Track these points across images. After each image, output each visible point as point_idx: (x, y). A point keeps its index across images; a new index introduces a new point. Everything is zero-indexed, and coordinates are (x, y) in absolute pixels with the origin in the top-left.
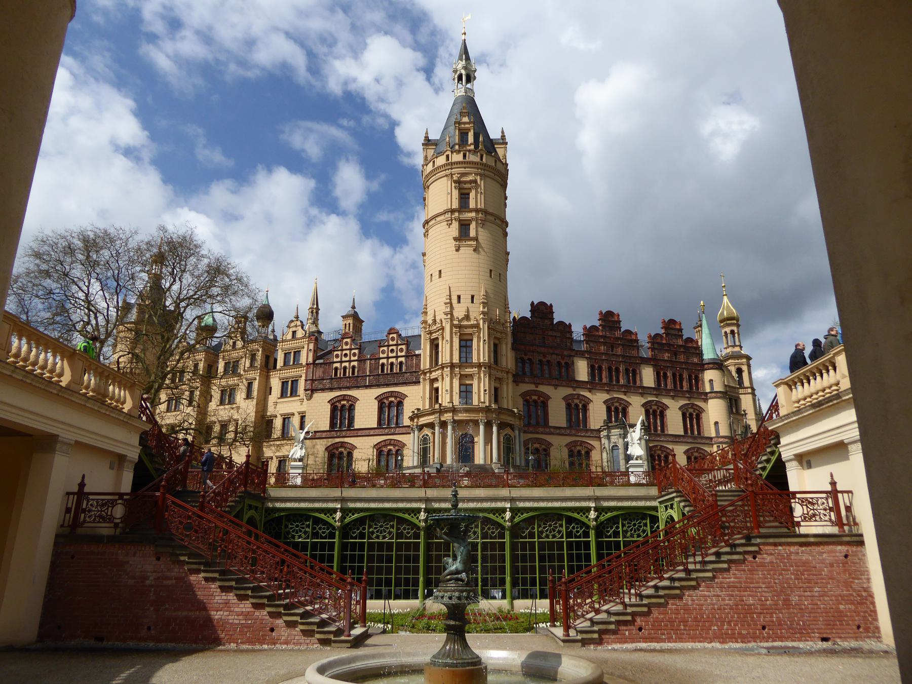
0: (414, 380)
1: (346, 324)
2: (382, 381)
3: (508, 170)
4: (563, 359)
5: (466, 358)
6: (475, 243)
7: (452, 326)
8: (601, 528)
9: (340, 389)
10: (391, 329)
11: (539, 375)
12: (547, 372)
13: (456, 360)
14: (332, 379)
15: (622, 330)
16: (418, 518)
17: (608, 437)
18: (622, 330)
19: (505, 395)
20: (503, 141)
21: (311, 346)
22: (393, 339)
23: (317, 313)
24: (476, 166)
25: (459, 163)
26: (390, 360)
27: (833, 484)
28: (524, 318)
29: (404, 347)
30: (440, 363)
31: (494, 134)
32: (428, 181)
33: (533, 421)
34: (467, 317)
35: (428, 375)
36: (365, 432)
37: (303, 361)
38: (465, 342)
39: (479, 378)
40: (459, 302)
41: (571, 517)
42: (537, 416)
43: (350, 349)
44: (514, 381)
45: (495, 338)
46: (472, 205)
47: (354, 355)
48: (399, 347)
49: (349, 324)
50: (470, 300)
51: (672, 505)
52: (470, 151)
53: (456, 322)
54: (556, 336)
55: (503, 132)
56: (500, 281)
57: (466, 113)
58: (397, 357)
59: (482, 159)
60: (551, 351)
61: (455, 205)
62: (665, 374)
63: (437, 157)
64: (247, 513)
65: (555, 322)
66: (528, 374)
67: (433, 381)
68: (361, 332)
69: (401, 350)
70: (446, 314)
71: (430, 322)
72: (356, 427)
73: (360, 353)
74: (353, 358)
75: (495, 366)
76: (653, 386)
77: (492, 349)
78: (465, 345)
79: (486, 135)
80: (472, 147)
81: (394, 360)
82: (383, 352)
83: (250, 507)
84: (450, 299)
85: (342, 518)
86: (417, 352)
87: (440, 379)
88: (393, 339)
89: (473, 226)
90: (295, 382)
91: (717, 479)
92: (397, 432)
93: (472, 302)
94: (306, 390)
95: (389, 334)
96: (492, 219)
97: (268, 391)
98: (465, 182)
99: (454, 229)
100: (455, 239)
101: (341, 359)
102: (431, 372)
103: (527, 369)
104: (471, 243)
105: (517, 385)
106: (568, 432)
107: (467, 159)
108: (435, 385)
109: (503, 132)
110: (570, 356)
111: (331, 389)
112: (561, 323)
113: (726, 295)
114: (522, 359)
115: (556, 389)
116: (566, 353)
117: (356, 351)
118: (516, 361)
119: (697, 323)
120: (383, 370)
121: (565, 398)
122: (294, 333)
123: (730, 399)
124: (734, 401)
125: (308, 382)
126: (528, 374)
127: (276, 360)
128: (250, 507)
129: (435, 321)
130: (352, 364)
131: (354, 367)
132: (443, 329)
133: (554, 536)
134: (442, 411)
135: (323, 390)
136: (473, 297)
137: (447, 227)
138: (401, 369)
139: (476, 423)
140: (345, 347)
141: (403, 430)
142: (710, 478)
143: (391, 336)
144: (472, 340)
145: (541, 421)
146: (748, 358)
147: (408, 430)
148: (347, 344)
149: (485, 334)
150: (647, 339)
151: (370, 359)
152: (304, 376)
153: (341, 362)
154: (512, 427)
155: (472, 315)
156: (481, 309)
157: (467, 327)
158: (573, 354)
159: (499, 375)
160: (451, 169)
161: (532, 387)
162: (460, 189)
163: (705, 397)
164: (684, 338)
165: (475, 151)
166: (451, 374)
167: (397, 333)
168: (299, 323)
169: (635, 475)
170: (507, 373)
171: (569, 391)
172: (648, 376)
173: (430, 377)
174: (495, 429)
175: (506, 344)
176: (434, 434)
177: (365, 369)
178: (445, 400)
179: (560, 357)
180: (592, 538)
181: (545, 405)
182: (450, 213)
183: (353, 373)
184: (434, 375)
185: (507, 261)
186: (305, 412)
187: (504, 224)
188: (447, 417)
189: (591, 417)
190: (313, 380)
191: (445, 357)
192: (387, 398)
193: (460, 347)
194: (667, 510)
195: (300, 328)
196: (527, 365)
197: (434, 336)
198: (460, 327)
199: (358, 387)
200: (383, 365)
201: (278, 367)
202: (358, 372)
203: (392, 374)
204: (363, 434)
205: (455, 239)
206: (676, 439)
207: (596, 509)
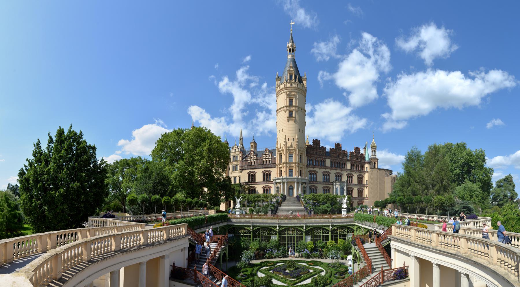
2: (264, 166)
7: (286, 149)
9: (251, 169)
10: (266, 149)
12: (317, 164)
13: (288, 161)
17: (335, 185)
21: (241, 155)
22: (267, 152)
26: (266, 160)
29: (270, 155)
33: (312, 180)
34: (291, 146)
37: (239, 159)
39: (295, 167)
40: (289, 141)
42: (314, 178)
43: (253, 156)
44: (307, 167)
53: (288, 148)
60: (319, 156)
66: (311, 164)
67: (280, 168)
69: (270, 156)
70: (284, 145)
71: (279, 147)
72: (256, 181)
73: (256, 157)
74: (254, 159)
78: (291, 155)
81: (267, 159)
82: (264, 157)
84: (286, 140)
86: (275, 157)
87: (282, 167)
90: (236, 166)
93: (293, 141)
94: (240, 170)
102: (279, 165)
103: (311, 163)
104: (293, 119)
108: (281, 169)
110: (325, 158)
111: (248, 169)
112: (323, 147)
114: (309, 159)
116: (324, 157)
117: (255, 156)
118: (308, 160)
120: (264, 163)
121: (323, 172)
122: (235, 150)
126: (311, 164)
127: (230, 159)
129: (280, 147)
130: (254, 161)
131: (254, 162)
132: (283, 150)
133: (318, 234)
134: (283, 179)
135: (245, 169)
138: (270, 162)
139: (294, 182)
140: (251, 155)
141: (271, 183)
145: (315, 180)
147: (272, 183)
149: (297, 152)
151: (260, 159)
152: (239, 165)
153: (251, 160)
154: (305, 183)
155: (293, 146)
156: (296, 143)
157: (291, 150)
159: (302, 166)
161: (312, 169)
166: (286, 166)
168: (236, 147)
171: (324, 170)
175: (304, 155)
176: (280, 186)
177: (258, 162)
178: (284, 175)
180: (330, 234)
181: (316, 175)
183: (254, 164)
184: (281, 166)
186: (240, 176)
188: (285, 180)
190: (242, 166)
191: (284, 160)
192: (265, 172)
193: (289, 156)
196: (311, 161)
197: (280, 152)
198: (289, 150)
199: (256, 169)
200: (264, 161)
203: (267, 164)
207: (332, 226)
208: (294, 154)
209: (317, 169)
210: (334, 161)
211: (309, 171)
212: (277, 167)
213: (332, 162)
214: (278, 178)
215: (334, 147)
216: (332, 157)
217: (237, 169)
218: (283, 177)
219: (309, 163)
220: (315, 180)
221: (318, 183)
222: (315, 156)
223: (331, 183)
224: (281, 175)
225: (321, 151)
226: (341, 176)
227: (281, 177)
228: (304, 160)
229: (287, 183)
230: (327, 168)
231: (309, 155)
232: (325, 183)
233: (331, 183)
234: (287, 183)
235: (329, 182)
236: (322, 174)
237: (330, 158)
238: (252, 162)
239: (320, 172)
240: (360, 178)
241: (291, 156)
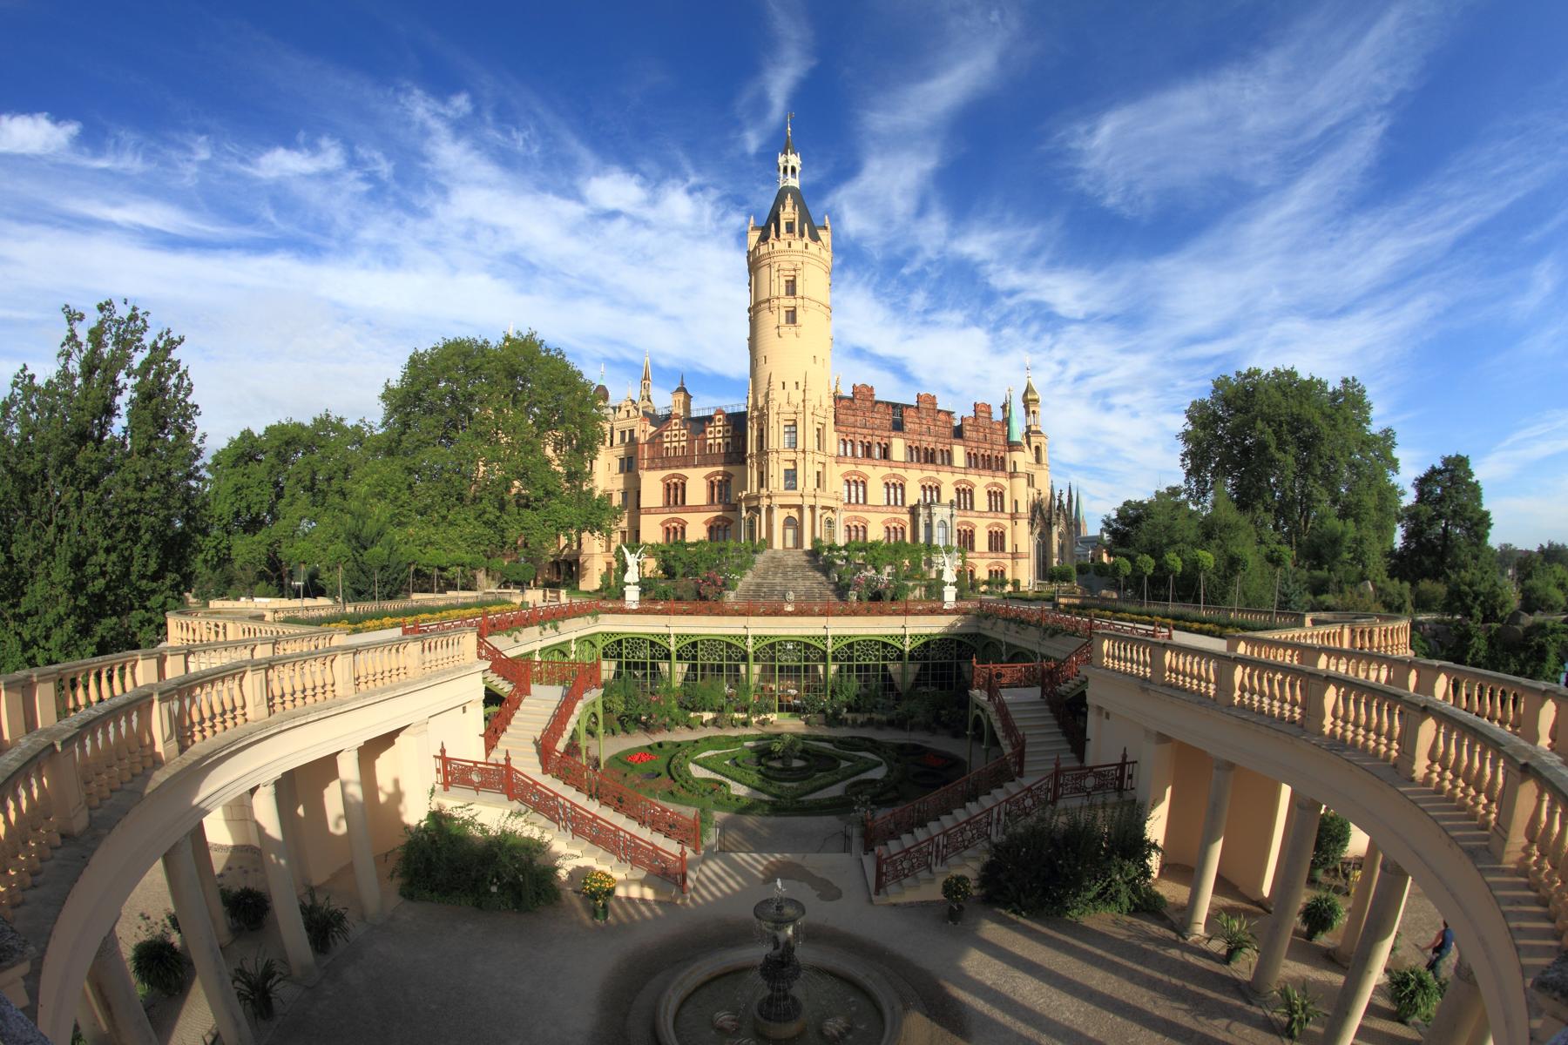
9: (670, 468)
27: (1125, 756)
33: (853, 500)
36: (696, 509)
60: (871, 432)
66: (849, 454)
74: (682, 438)
93: (797, 388)
106: (885, 509)
111: (662, 468)
114: (843, 440)
122: (628, 411)
126: (849, 454)
130: (682, 444)
131: (683, 447)
135: (654, 469)
136: (797, 383)
140: (674, 428)
143: (718, 417)
145: (861, 501)
153: (671, 442)
154: (832, 509)
161: (852, 468)
171: (887, 471)
199: (686, 466)
206: (981, 514)
209: (865, 469)
210: (917, 444)
213: (910, 447)
220: (861, 501)
222: (859, 431)
229: (782, 506)
230: (897, 464)
231: (844, 429)
236: (882, 483)
238: (675, 448)
239: (876, 474)
240: (996, 497)
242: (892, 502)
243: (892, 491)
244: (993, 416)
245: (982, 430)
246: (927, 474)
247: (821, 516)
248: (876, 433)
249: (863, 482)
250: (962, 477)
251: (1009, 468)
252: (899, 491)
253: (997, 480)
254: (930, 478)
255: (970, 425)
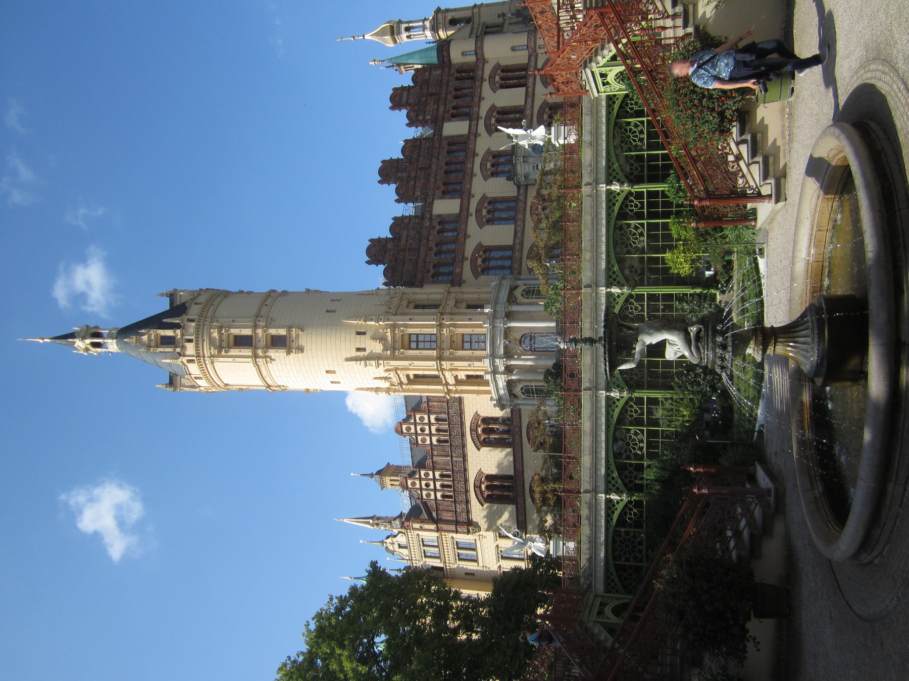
0: (458, 404)
1: (392, 485)
3: (207, 289)
4: (434, 227)
5: (431, 341)
6: (294, 330)
7: (394, 358)
8: (632, 177)
9: (467, 491)
10: (397, 431)
11: (453, 255)
14: (455, 501)
15: (401, 157)
16: (618, 400)
18: (401, 157)
19: (476, 296)
20: (172, 296)
21: (417, 526)
22: (408, 429)
23: (378, 519)
24: (201, 327)
25: (197, 347)
26: (434, 432)
28: (385, 273)
30: (437, 373)
31: (164, 305)
32: (219, 386)
33: (508, 263)
34: (382, 339)
35: (450, 388)
38: (412, 343)
39: (455, 326)
40: (364, 350)
41: (618, 213)
42: (501, 258)
43: (420, 479)
44: (460, 285)
45: (407, 307)
46: (247, 332)
47: (427, 475)
48: (418, 421)
49: (391, 480)
50: (363, 336)
51: (603, 76)
52: (182, 335)
54: (408, 235)
55: (162, 295)
56: (340, 300)
57: (136, 338)
58: (430, 424)
59: (192, 321)
61: (248, 352)
62: (454, 108)
63: (190, 374)
64: (608, 618)
65: (390, 236)
66: (451, 268)
67: (458, 382)
68: (400, 467)
69: (422, 419)
70: (378, 365)
74: (431, 476)
75: (441, 307)
76: (467, 123)
77: (421, 311)
79: (165, 314)
80: (178, 332)
82: (424, 440)
83: (600, 613)
85: (618, 492)
88: (408, 429)
89: (273, 332)
91: (569, 21)
92: (519, 425)
94: (468, 532)
95: (402, 433)
96: (264, 309)
97: (470, 577)
98: (221, 340)
99: (277, 354)
100: (289, 353)
101: (431, 490)
102: (447, 384)
105: (464, 282)
106: (519, 223)
107: (193, 337)
109: (162, 295)
110: (431, 219)
111: (468, 502)
112: (392, 229)
113: (364, 36)
114: (433, 276)
115: (469, 237)
116: (427, 223)
117: (423, 472)
118: (437, 282)
119: (396, 70)
121: (481, 225)
122: (400, 546)
123: (486, 33)
124: (487, 30)
125: (459, 529)
127: (434, 568)
128: (600, 613)
129: (386, 378)
132: (396, 369)
134: (495, 372)
135: (468, 512)
137: (273, 362)
142: (569, 29)
143: (405, 431)
144: (410, 335)
145: (509, 253)
146: (438, 11)
148: (414, 484)
150: (413, 128)
152: (454, 535)
154: (513, 289)
158: (429, 216)
159: (452, 303)
160: (204, 357)
161: (467, 265)
162: (229, 347)
163: (481, 59)
164: (412, 84)
165: (183, 328)
167: (401, 424)
168: (389, 540)
169: (569, 135)
170: (449, 293)
171: (472, 221)
172: (455, 128)
173: (453, 385)
174: (515, 308)
175: (414, 293)
178: (482, 367)
179: (432, 231)
181: (488, 249)
182: (257, 360)
183: (449, 476)
184: (451, 380)
185: (316, 291)
187: (272, 294)
188: (500, 364)
189: (504, 195)
192: (478, 436)
193: (417, 348)
194: (608, 83)
195: (395, 540)
196: (442, 270)
197: (404, 380)
199: (465, 470)
201: (441, 565)
202: (447, 470)
204: (521, 464)
205: (289, 353)
206: (530, 96)
208: (410, 331)
210: (440, 183)
211: (476, 275)
212: (456, 392)
214: (491, 388)
215: (393, 187)
216: (427, 195)
217: (470, 544)
218: (487, 372)
219: (446, 278)
220: (509, 253)
221: (517, 241)
223: (522, 191)
224: (481, 377)
225: (405, 233)
226: (494, 157)
227: (488, 377)
228: (432, 296)
229: (508, 355)
230: (464, 208)
232: (520, 216)
233: (522, 191)
234: (508, 355)
235: (515, 199)
236: (488, 228)
237: (429, 200)
241: (417, 342)
242: (513, 213)
243: (497, 214)
244: (406, 85)
245: (424, 99)
246: (477, 169)
247: (521, 304)
248: (426, 236)
249: (485, 252)
250: (481, 123)
251: (472, 59)
252: (499, 206)
253: (486, 75)
254: (483, 165)
255: (417, 116)
